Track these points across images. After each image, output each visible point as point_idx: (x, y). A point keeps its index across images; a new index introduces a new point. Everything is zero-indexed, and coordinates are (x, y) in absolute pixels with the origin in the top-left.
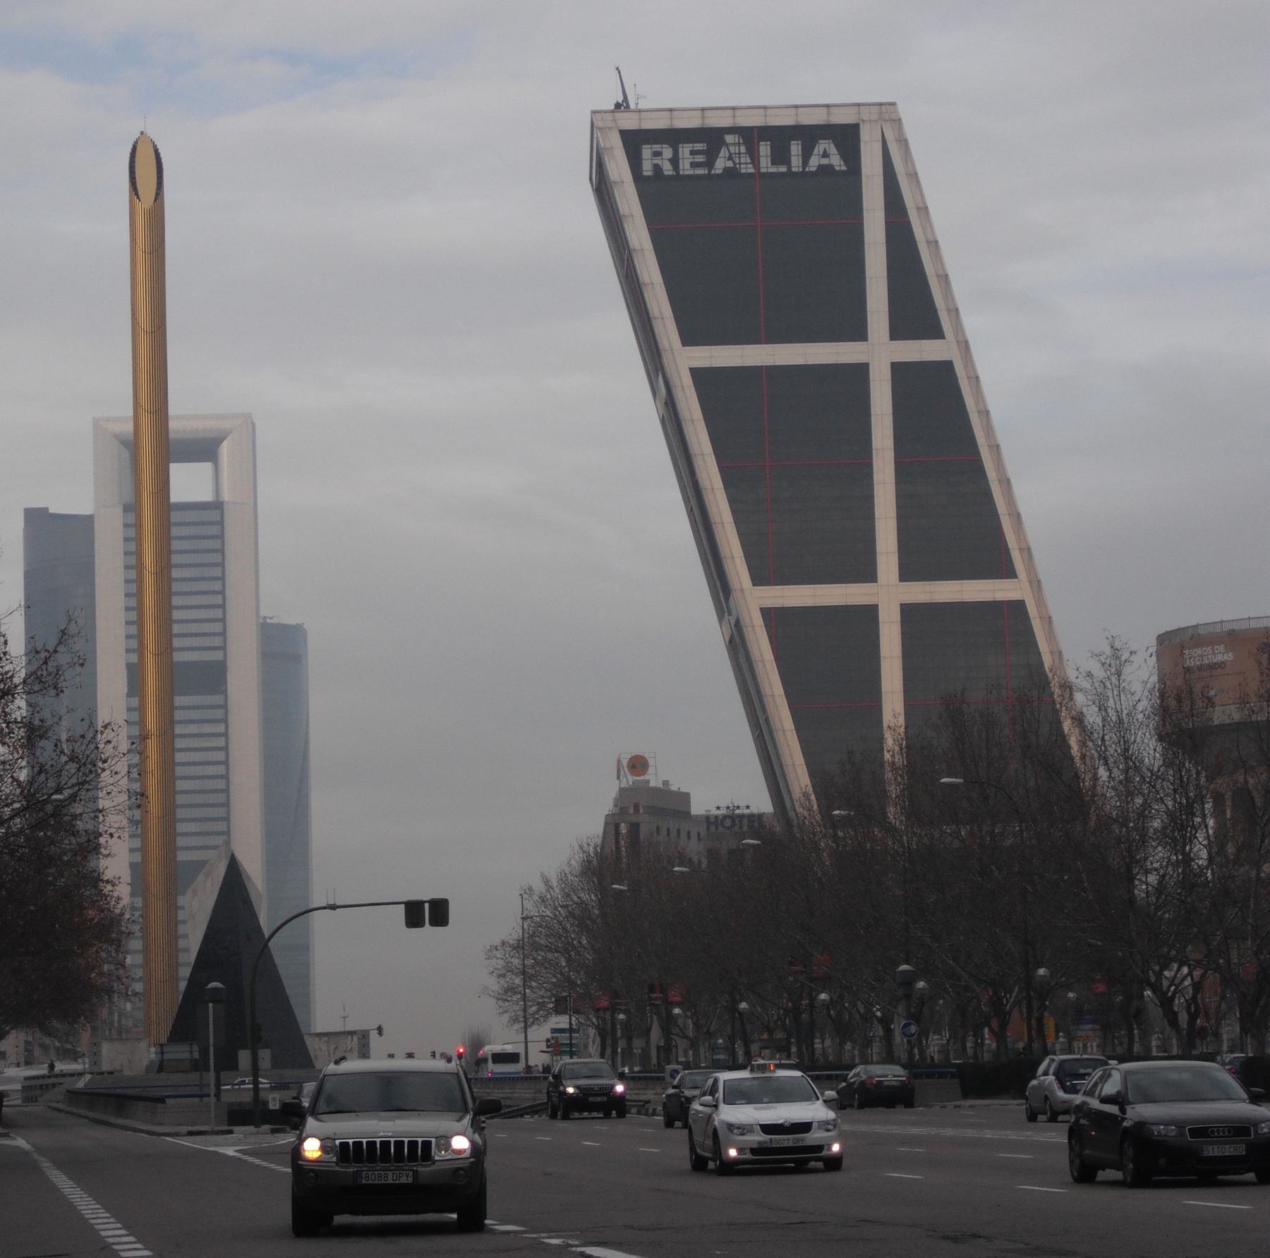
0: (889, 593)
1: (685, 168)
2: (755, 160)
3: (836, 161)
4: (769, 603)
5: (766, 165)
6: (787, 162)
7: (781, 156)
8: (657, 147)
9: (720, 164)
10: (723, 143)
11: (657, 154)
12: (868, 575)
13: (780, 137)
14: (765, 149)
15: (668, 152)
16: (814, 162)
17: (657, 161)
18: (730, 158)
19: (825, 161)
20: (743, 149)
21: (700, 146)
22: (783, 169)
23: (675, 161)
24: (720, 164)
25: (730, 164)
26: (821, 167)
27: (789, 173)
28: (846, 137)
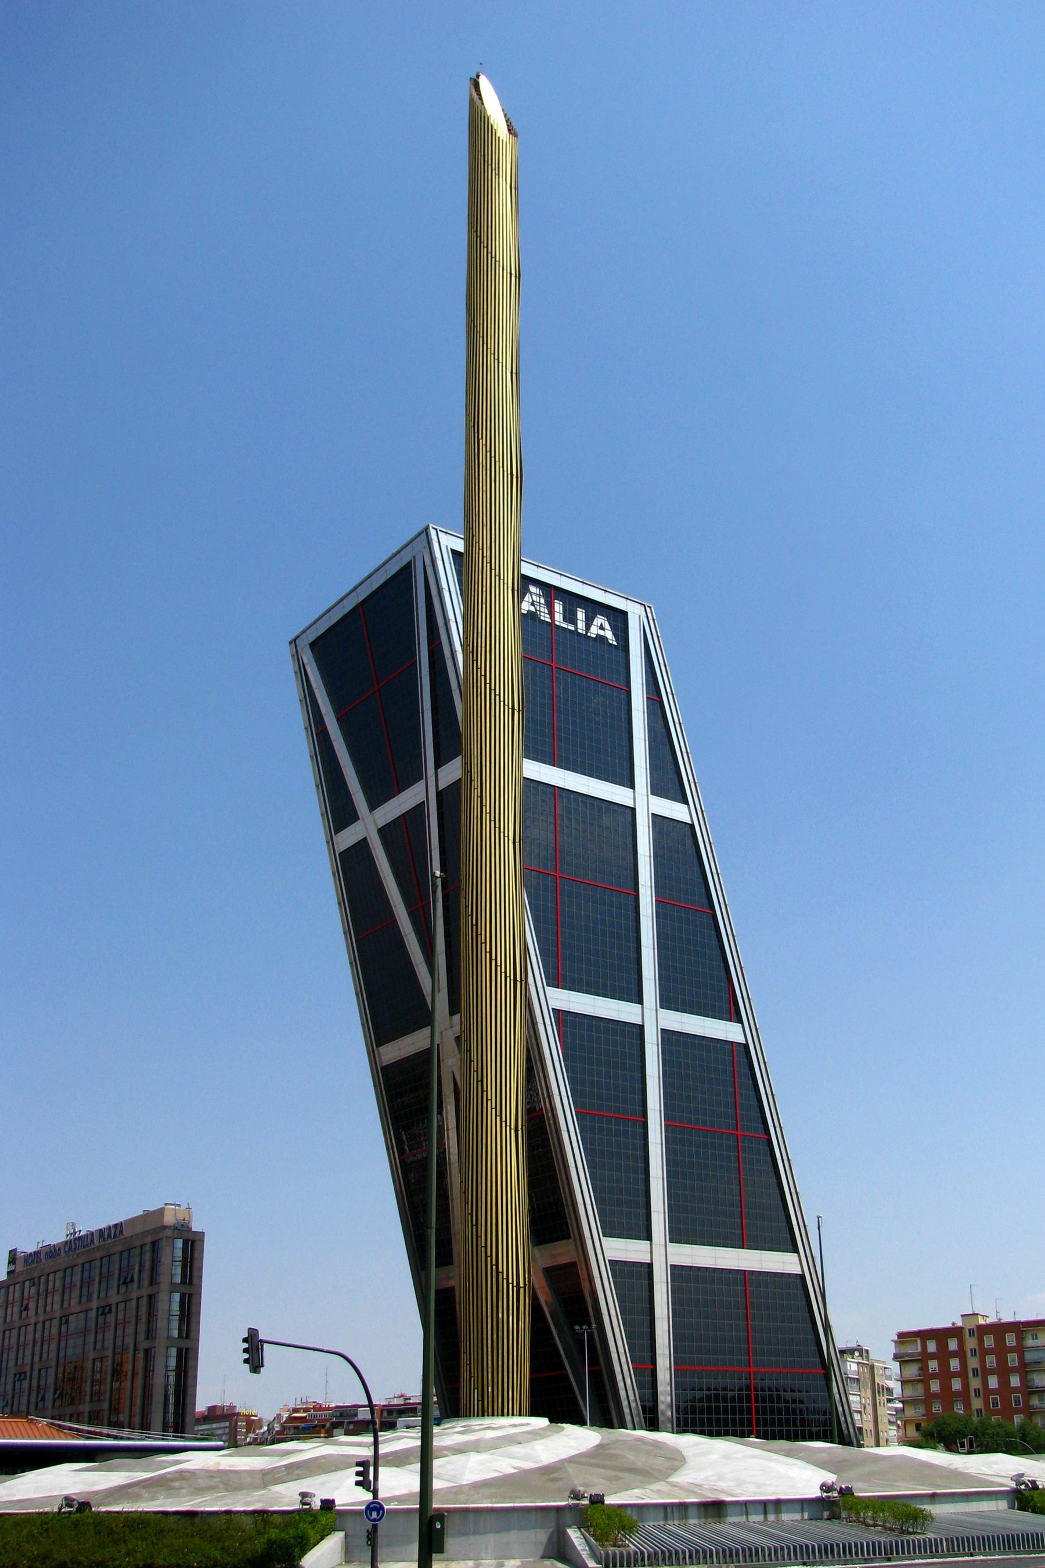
2: (551, 613)
3: (609, 634)
5: (559, 618)
14: (558, 607)
16: (594, 631)
18: (533, 604)
19: (601, 633)
20: (542, 601)
25: (532, 609)
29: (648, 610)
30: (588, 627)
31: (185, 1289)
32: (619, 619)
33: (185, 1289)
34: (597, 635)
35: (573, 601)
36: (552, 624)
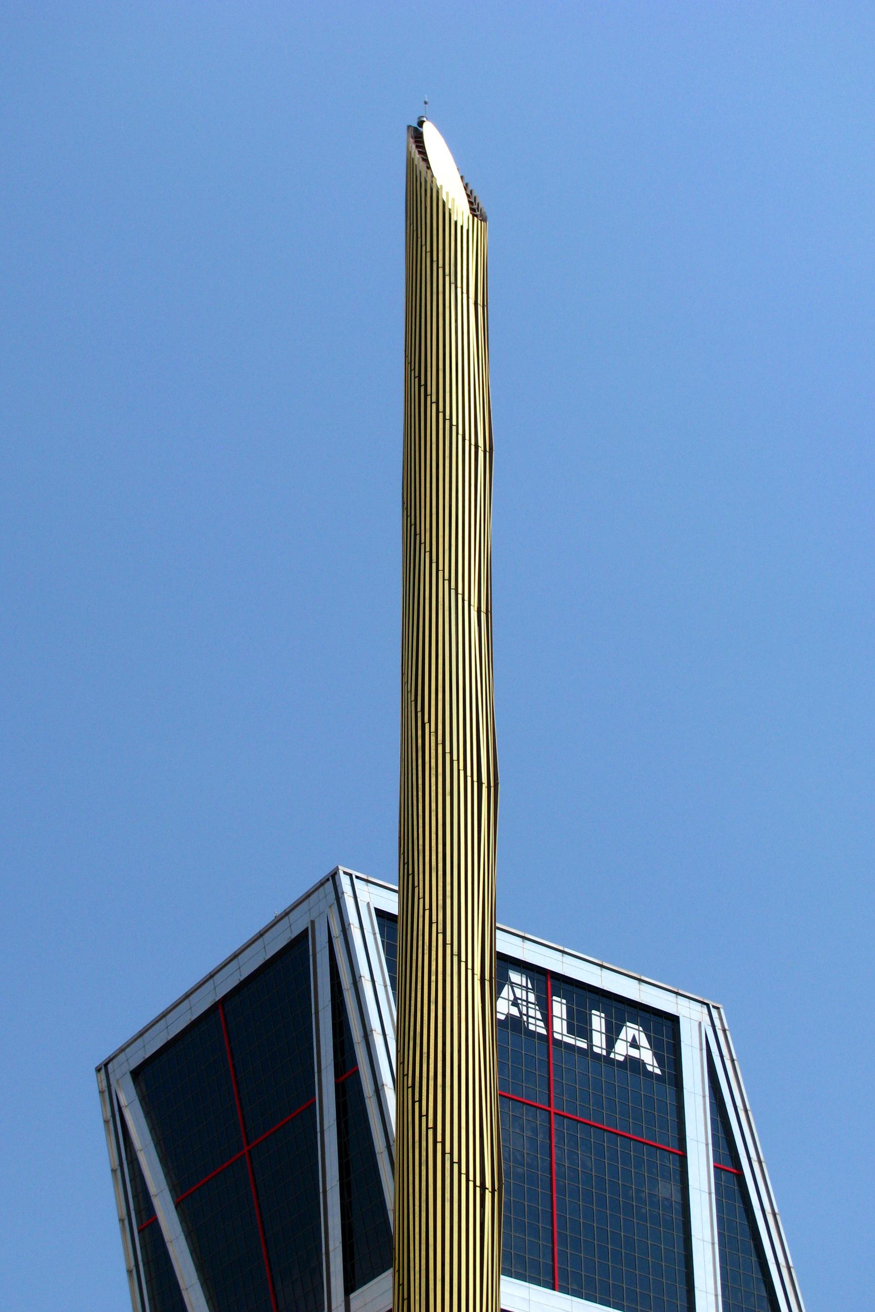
2: (548, 1019)
3: (647, 1056)
7: (579, 1025)
14: (559, 1008)
16: (621, 1050)
18: (515, 1003)
19: (633, 1053)
20: (532, 998)
25: (514, 1011)
27: (589, 1052)
29: (714, 1013)
30: (611, 1044)
32: (664, 1028)
34: (627, 1057)
35: (583, 997)
36: (548, 1039)
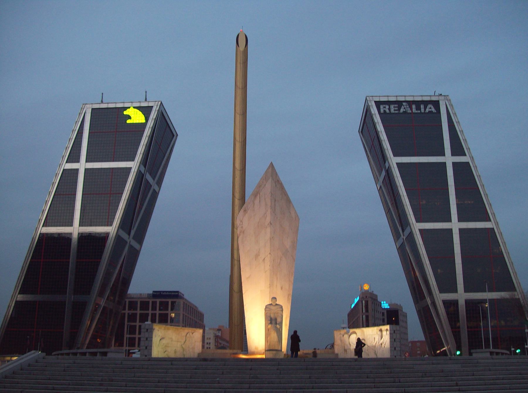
0: (455, 225)
1: (392, 111)
2: (411, 109)
3: (433, 110)
4: (421, 228)
5: (414, 110)
6: (420, 110)
8: (384, 106)
9: (402, 110)
10: (402, 105)
11: (385, 107)
12: (449, 220)
13: (418, 104)
14: (414, 107)
15: (387, 107)
16: (427, 110)
17: (385, 109)
19: (430, 110)
21: (396, 106)
22: (419, 112)
23: (389, 109)
24: (402, 110)
26: (429, 111)
28: (436, 104)
31: (367, 314)
33: (367, 314)
36: (412, 113)
